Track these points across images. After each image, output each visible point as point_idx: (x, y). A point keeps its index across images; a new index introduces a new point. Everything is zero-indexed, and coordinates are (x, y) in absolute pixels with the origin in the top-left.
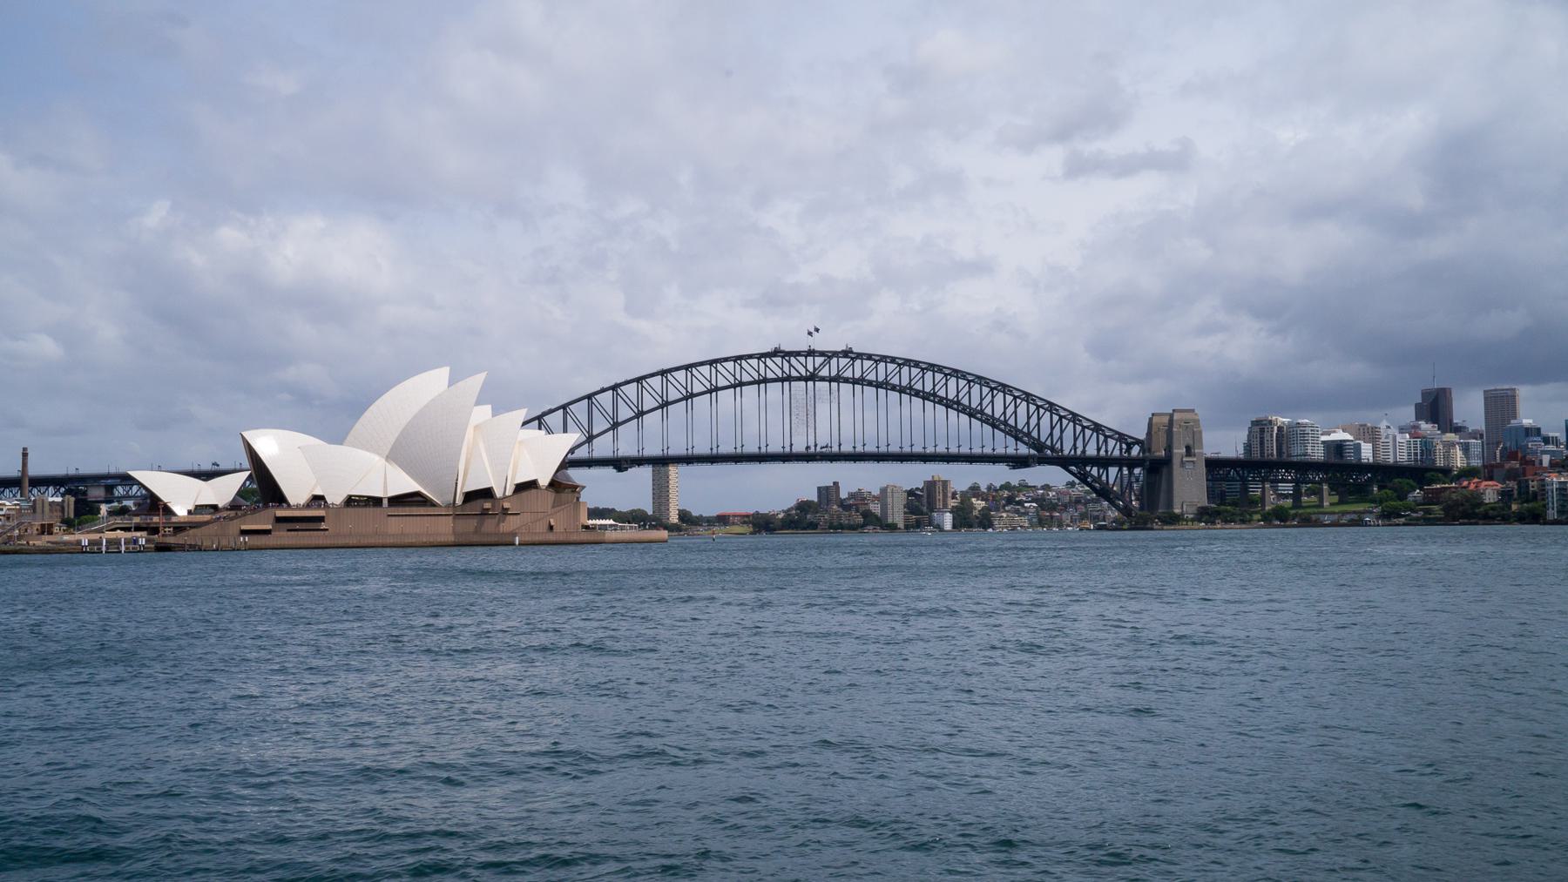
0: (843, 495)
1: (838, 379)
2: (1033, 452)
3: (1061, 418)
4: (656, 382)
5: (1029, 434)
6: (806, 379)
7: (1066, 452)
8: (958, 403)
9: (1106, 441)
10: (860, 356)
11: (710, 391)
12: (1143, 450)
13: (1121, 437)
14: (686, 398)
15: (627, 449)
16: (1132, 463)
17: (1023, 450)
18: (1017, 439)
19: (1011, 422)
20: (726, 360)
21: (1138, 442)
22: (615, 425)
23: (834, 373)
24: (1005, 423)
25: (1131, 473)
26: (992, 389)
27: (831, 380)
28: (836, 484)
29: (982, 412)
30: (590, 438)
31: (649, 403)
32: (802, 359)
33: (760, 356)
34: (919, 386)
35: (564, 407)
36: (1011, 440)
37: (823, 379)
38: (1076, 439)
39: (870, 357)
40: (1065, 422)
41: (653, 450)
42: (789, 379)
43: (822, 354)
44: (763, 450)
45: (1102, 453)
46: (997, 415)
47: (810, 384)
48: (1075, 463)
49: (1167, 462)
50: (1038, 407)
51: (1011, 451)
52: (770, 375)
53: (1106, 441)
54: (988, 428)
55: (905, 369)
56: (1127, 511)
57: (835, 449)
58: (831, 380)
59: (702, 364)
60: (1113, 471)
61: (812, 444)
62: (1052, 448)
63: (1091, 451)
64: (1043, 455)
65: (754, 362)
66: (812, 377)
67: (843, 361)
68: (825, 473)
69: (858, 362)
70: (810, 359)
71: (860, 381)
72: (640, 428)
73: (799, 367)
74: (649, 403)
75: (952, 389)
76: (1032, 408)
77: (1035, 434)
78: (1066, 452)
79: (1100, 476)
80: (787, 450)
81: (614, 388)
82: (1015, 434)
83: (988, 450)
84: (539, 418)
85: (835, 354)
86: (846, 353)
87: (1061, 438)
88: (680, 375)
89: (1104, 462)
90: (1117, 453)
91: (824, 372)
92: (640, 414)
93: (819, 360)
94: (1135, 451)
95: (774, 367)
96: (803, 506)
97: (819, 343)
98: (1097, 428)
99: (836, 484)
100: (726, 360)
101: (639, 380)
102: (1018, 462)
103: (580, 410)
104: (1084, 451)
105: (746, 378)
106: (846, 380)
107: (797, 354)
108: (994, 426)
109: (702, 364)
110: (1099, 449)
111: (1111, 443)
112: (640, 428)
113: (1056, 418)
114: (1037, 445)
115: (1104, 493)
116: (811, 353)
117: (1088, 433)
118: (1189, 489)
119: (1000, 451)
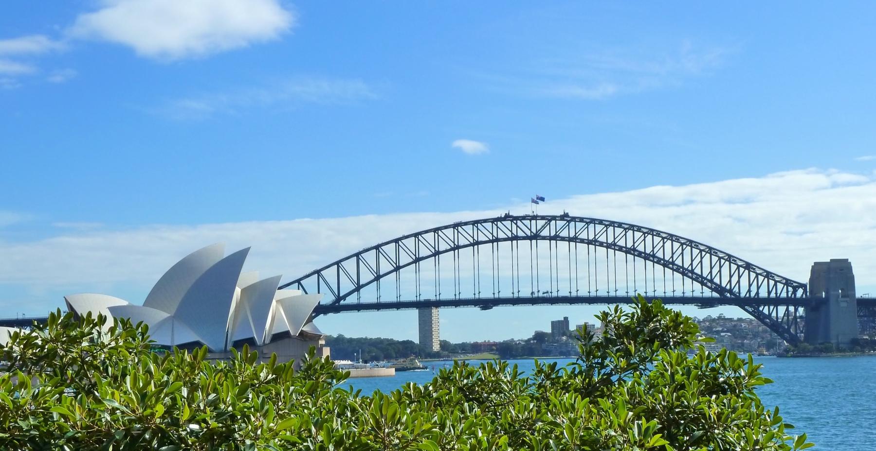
0: (572, 327)
1: (556, 238)
2: (716, 295)
3: (739, 267)
4: (410, 243)
5: (711, 281)
6: (530, 238)
7: (743, 295)
8: (654, 256)
9: (775, 285)
10: (574, 219)
11: (453, 249)
12: (805, 291)
13: (788, 283)
14: (434, 255)
15: (388, 297)
16: (796, 302)
17: (708, 293)
18: (703, 284)
19: (698, 271)
20: (466, 224)
21: (803, 286)
22: (378, 278)
23: (553, 234)
24: (692, 271)
25: (796, 310)
26: (682, 244)
27: (551, 238)
28: (566, 319)
29: (673, 263)
30: (358, 288)
31: (404, 259)
32: (527, 222)
33: (494, 221)
34: (622, 243)
35: (338, 263)
36: (697, 286)
37: (544, 238)
38: (750, 285)
39: (581, 220)
40: (742, 270)
41: (408, 296)
42: (516, 238)
43: (543, 218)
44: (496, 296)
45: (773, 295)
46: (686, 266)
47: (534, 241)
48: (750, 303)
49: (826, 301)
50: (720, 258)
51: (697, 294)
52: (501, 235)
53: (775, 285)
54: (678, 276)
55: (611, 229)
56: (793, 340)
57: (555, 294)
58: (551, 238)
59: (446, 227)
60: (782, 309)
61: (535, 290)
62: (731, 291)
63: (763, 294)
64: (725, 296)
65: (488, 225)
66: (535, 237)
67: (560, 223)
68: (558, 312)
69: (572, 224)
70: (533, 222)
71: (574, 239)
72: (398, 279)
73: (524, 229)
74: (404, 259)
75: (647, 245)
76: (715, 259)
77: (717, 280)
78: (743, 295)
79: (770, 314)
80: (516, 295)
81: (377, 247)
82: (701, 280)
83: (678, 294)
84: (298, 281)
85: (554, 218)
86: (564, 217)
87: (739, 282)
88: (430, 237)
89: (777, 302)
90: (784, 295)
91: (545, 233)
92: (397, 268)
93: (541, 223)
94: (800, 293)
95: (505, 229)
96: (540, 337)
97: (542, 209)
98: (769, 275)
99: (566, 319)
100: (466, 224)
101: (396, 241)
102: (705, 303)
103: (350, 265)
104: (757, 293)
105: (482, 238)
106: (563, 239)
107: (524, 218)
108: (683, 274)
109: (446, 227)
110: (769, 293)
111: (780, 286)
112: (398, 279)
113: (734, 267)
114: (719, 289)
115: (775, 326)
116: (535, 218)
117: (761, 278)
118: (843, 324)
119: (688, 294)
